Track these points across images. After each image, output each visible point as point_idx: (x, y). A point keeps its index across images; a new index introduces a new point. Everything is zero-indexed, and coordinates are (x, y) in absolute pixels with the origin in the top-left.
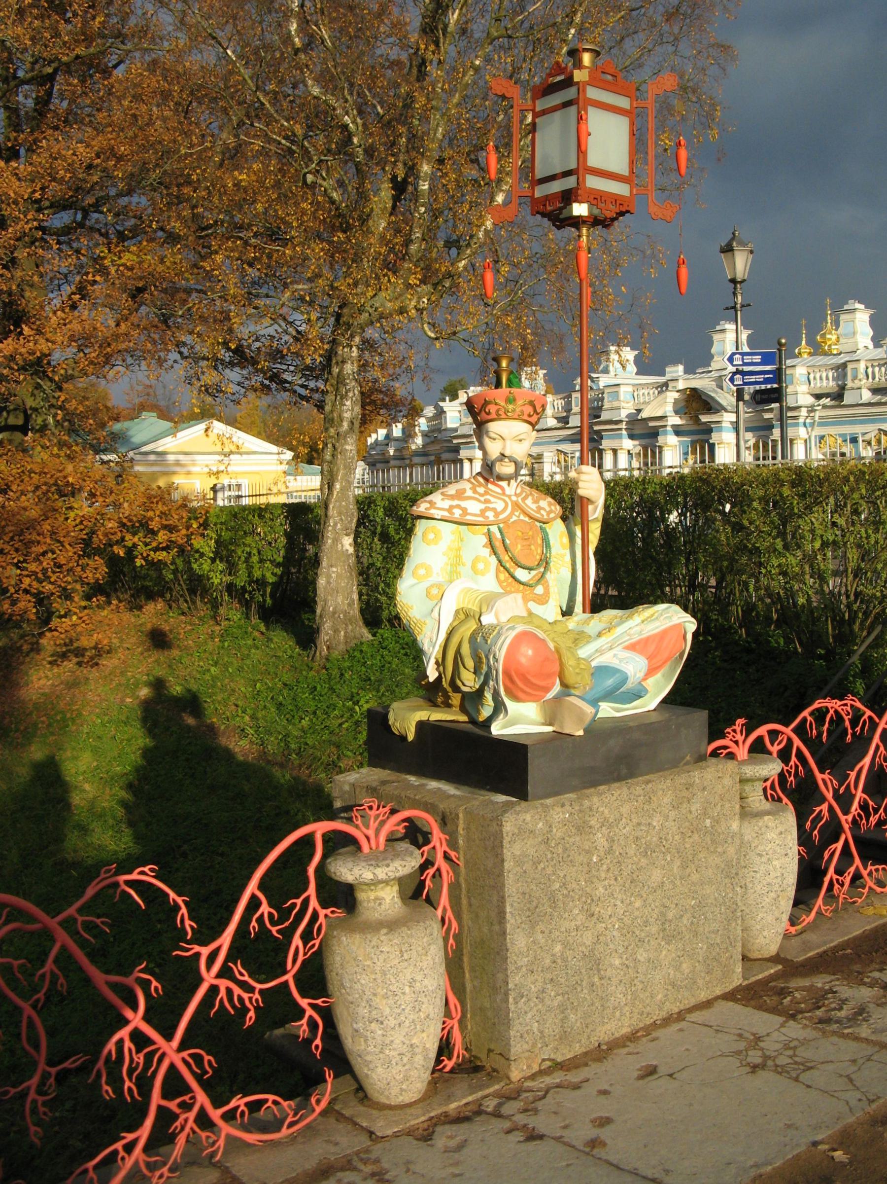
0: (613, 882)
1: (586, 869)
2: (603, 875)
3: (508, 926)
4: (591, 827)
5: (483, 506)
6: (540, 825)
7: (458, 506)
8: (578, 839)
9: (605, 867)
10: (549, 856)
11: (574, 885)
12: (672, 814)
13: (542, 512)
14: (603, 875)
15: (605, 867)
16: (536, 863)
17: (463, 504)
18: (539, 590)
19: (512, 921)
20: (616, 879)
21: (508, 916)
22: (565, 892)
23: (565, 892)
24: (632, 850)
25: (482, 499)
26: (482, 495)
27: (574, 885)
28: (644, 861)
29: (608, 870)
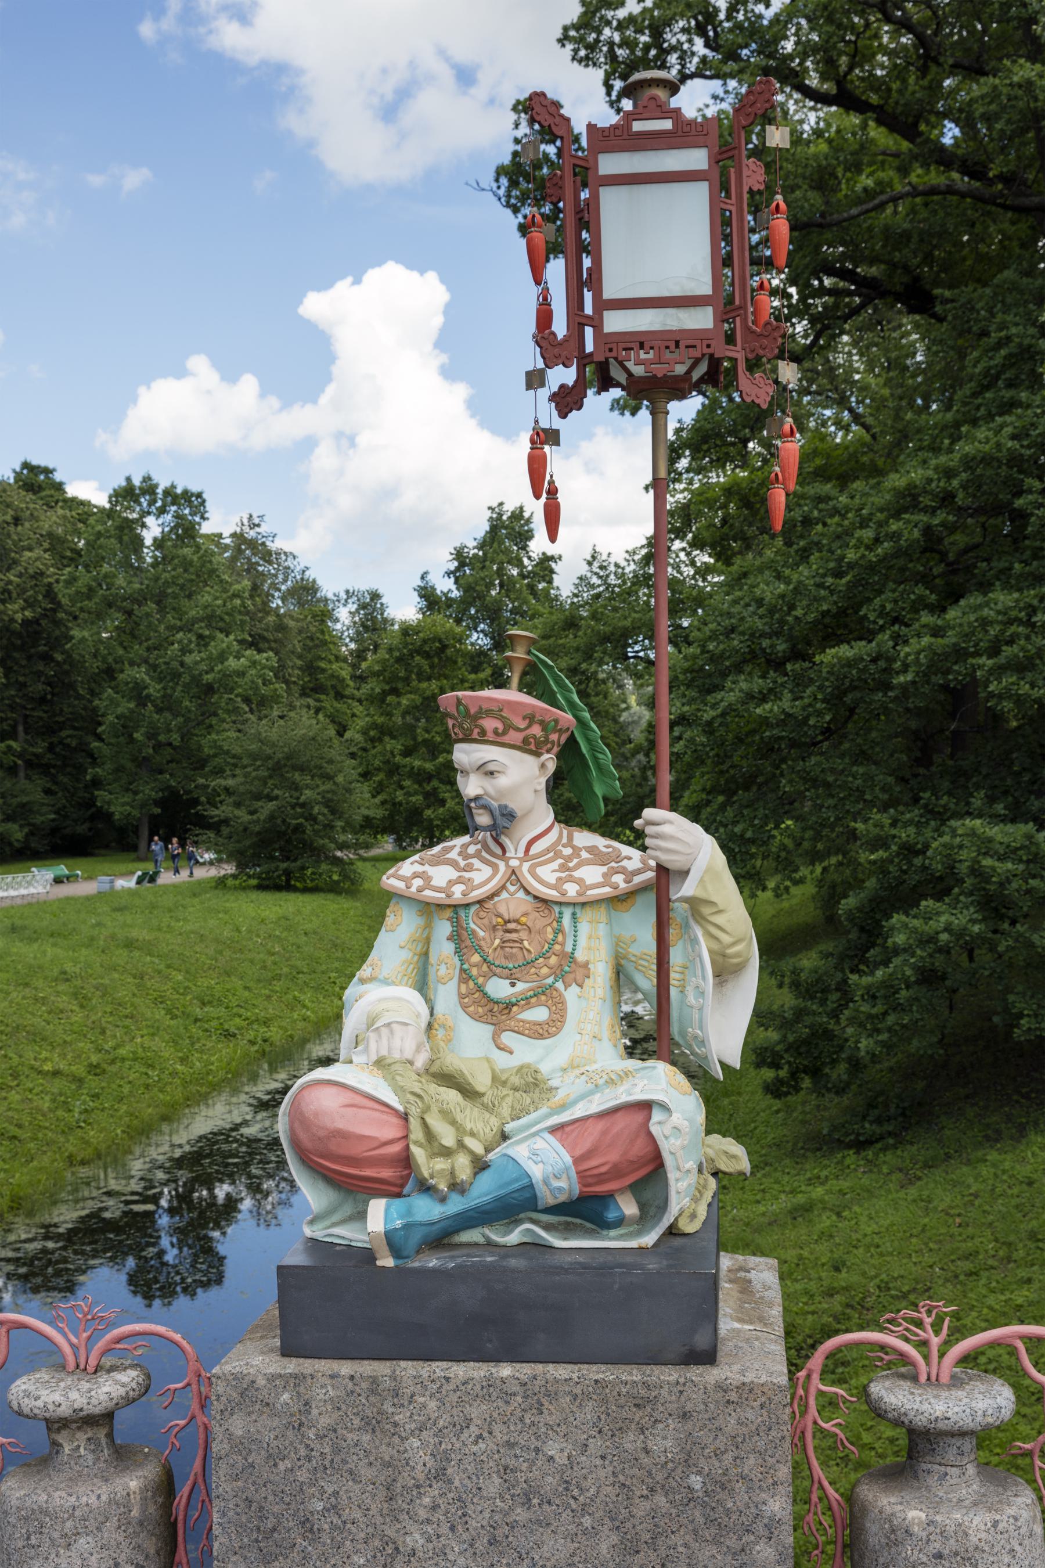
0: (445, 1529)
1: (382, 1493)
2: (423, 1514)
3: (216, 1545)
4: (396, 1424)
5: (454, 874)
6: (286, 1396)
8: (366, 1438)
9: (427, 1500)
10: (303, 1452)
11: (357, 1514)
12: (596, 1445)
14: (423, 1514)
15: (427, 1500)
16: (273, 1458)
18: (539, 1014)
19: (222, 1539)
20: (452, 1528)
21: (216, 1530)
22: (336, 1520)
23: (336, 1520)
24: (493, 1485)
25: (462, 863)
26: (467, 858)
27: (357, 1514)
28: (521, 1514)
29: (435, 1507)
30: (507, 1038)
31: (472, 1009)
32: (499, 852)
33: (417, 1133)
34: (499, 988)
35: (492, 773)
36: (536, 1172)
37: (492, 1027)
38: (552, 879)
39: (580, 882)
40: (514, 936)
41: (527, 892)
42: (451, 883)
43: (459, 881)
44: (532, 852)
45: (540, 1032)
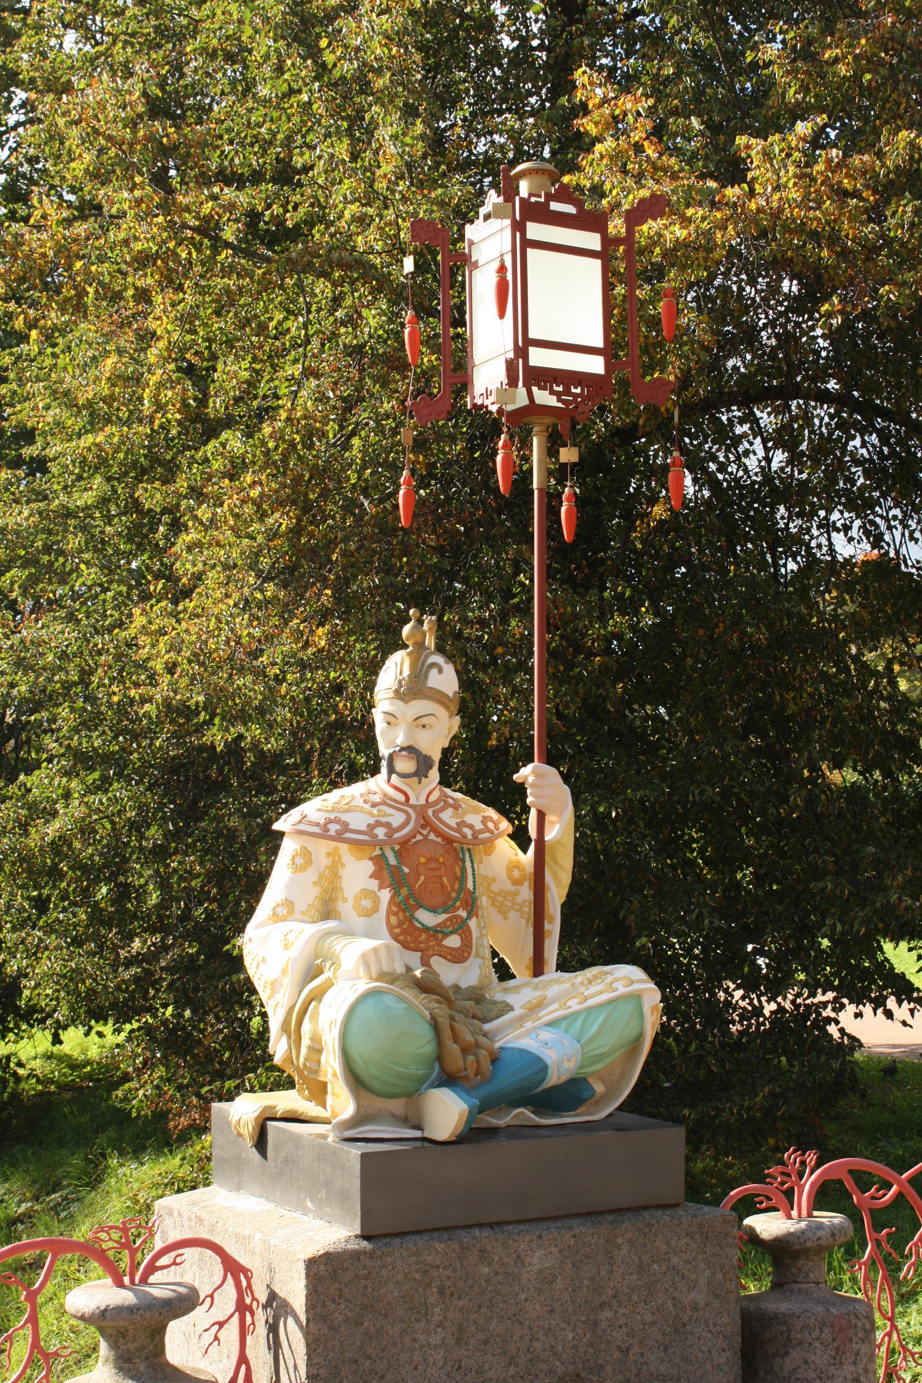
5: (372, 821)
7: (336, 821)
13: (466, 830)
17: (344, 817)
18: (454, 941)
30: (437, 963)
31: (402, 938)
32: (402, 798)
33: (447, 1034)
34: (426, 918)
35: (424, 726)
36: (550, 1056)
37: (419, 954)
38: (452, 822)
39: (471, 827)
40: (437, 873)
41: (439, 833)
42: (371, 827)
43: (378, 824)
44: (431, 799)
45: (458, 957)
